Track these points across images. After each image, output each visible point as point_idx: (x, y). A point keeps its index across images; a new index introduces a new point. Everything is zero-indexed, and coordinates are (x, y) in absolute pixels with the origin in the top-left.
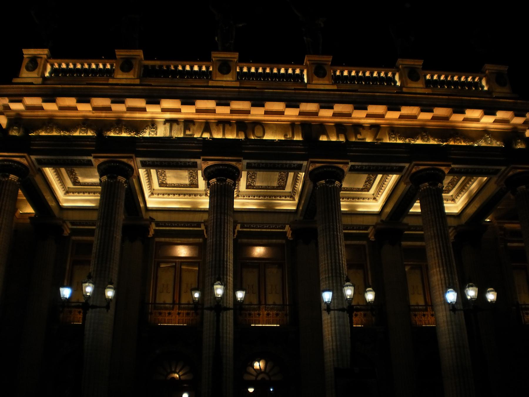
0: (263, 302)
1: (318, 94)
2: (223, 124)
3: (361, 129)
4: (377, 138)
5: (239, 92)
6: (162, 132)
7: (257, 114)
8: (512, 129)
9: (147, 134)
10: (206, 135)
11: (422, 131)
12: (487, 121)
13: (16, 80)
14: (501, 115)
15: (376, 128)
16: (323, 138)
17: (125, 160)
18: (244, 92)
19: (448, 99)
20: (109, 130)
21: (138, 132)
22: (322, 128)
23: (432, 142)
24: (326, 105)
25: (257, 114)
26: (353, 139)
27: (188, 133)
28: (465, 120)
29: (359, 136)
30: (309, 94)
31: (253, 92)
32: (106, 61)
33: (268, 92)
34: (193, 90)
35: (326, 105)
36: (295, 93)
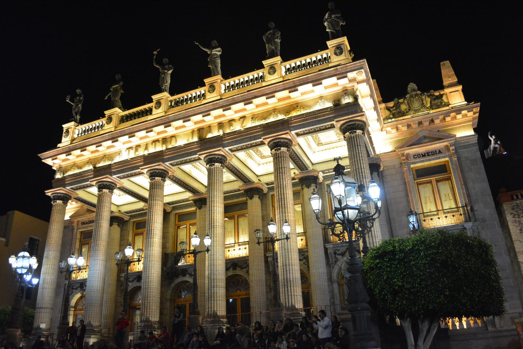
0: (237, 242)
1: (199, 108)
2: (155, 142)
3: (233, 122)
4: (244, 125)
5: (156, 121)
6: (125, 156)
7: (171, 131)
8: (343, 88)
9: (117, 159)
10: (146, 153)
11: (275, 111)
12: (320, 90)
13: (59, 145)
14: (326, 82)
15: (244, 117)
16: (209, 136)
17: (104, 180)
18: (159, 120)
19: (283, 84)
20: (100, 163)
21: (112, 160)
22: (209, 128)
23: (281, 117)
24: (206, 114)
25: (171, 131)
26: (228, 131)
27: (137, 153)
28: (302, 94)
29: (232, 128)
30: (194, 110)
31: (163, 119)
32: (102, 119)
33: (171, 117)
34: (132, 128)
35: (206, 114)
36: (186, 112)
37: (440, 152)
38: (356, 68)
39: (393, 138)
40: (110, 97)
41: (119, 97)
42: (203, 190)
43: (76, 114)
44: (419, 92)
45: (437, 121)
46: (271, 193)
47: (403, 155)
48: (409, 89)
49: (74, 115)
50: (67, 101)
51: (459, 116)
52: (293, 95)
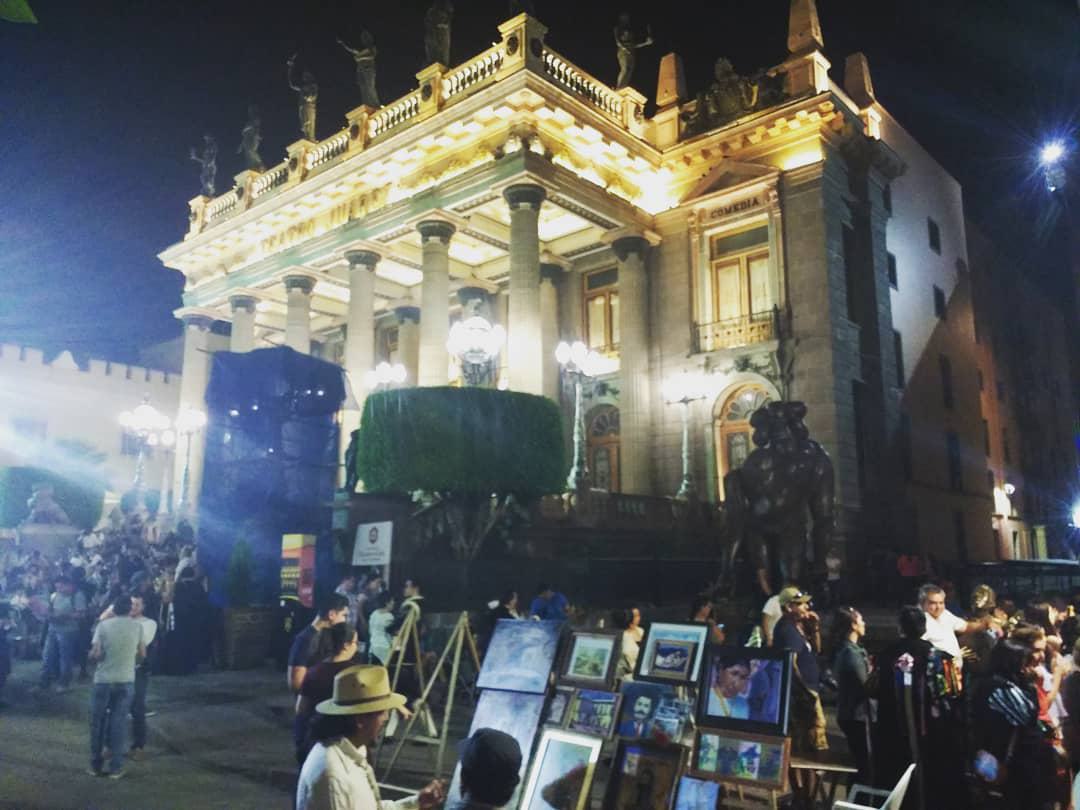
26: (372, 209)
37: (756, 202)
38: (516, 86)
39: (683, 180)
40: (244, 151)
41: (255, 148)
42: (342, 310)
43: (207, 181)
44: (735, 77)
45: (754, 139)
46: (505, 292)
47: (691, 214)
48: (718, 73)
49: (203, 181)
50: (193, 157)
51: (793, 124)
52: (443, 141)
